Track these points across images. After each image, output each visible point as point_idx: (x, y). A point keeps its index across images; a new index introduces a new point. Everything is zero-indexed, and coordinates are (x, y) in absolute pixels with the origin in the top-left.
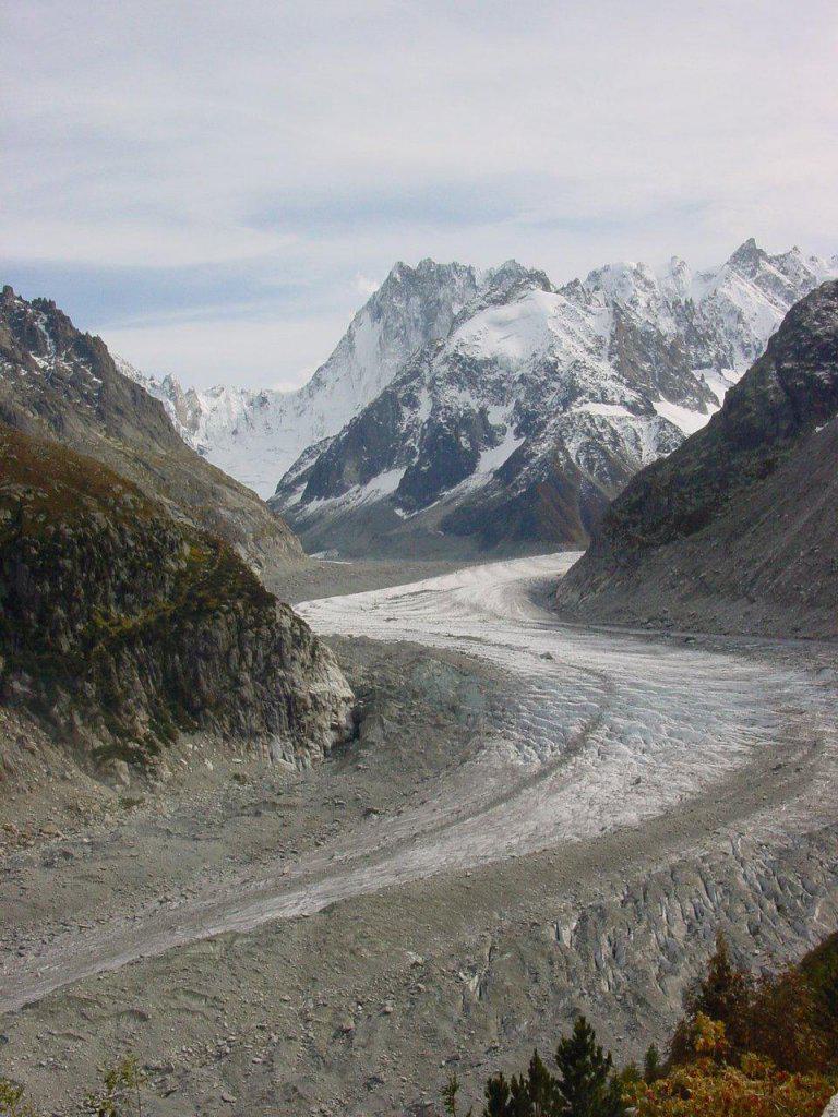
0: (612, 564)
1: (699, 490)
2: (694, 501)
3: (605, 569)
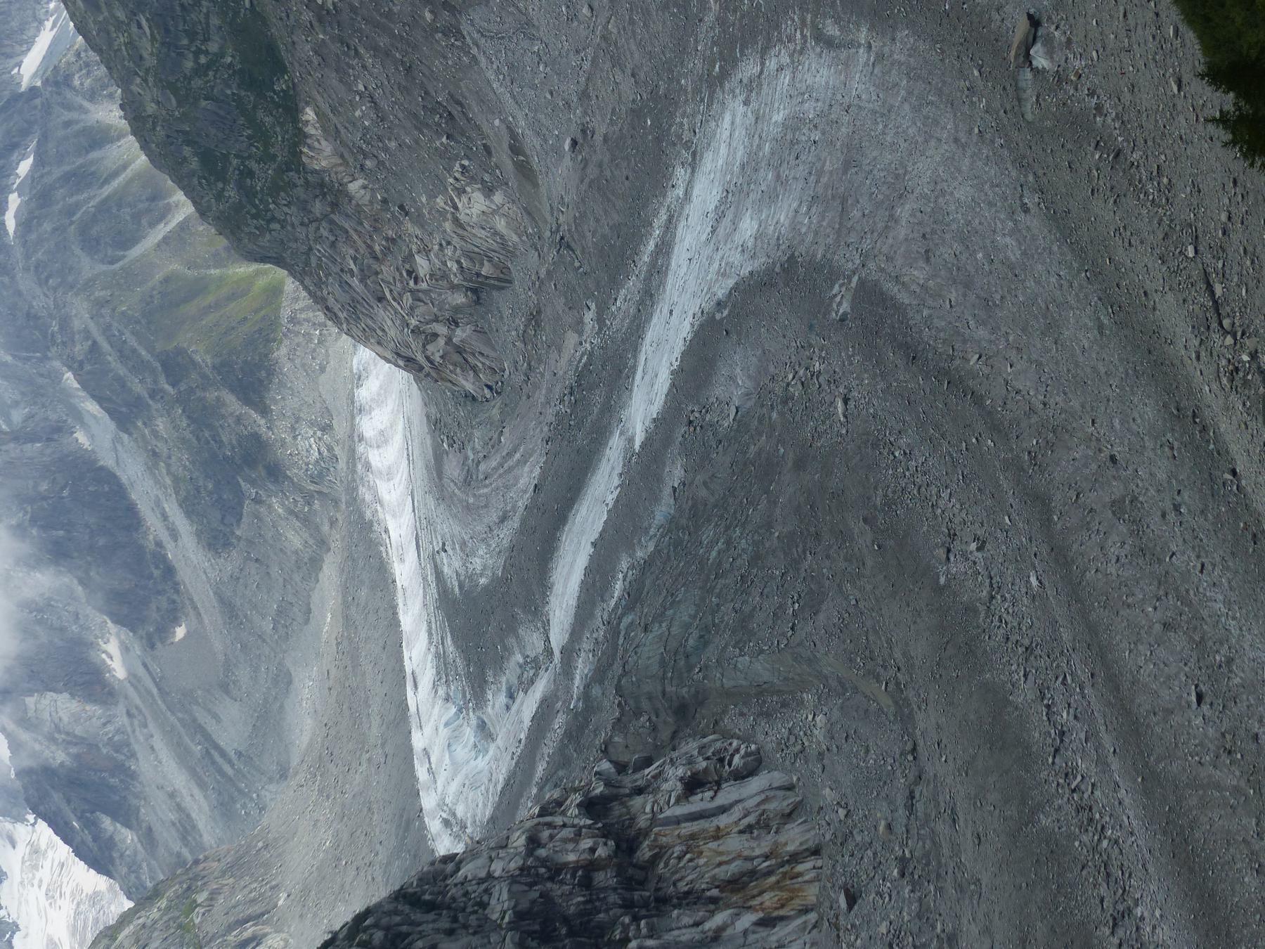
0: (325, 233)
1: (192, 35)
2: (213, 47)
3: (333, 245)
